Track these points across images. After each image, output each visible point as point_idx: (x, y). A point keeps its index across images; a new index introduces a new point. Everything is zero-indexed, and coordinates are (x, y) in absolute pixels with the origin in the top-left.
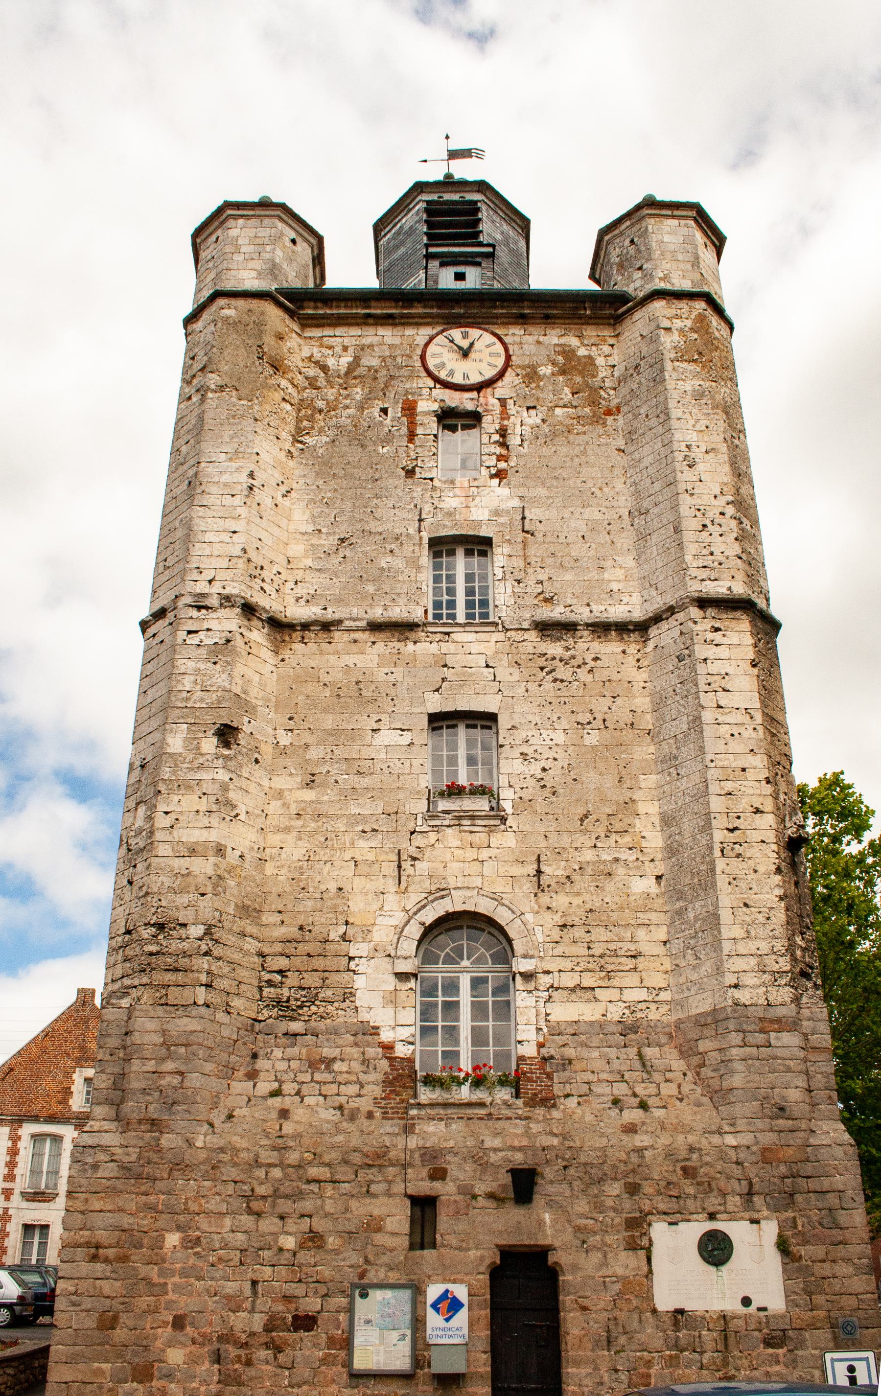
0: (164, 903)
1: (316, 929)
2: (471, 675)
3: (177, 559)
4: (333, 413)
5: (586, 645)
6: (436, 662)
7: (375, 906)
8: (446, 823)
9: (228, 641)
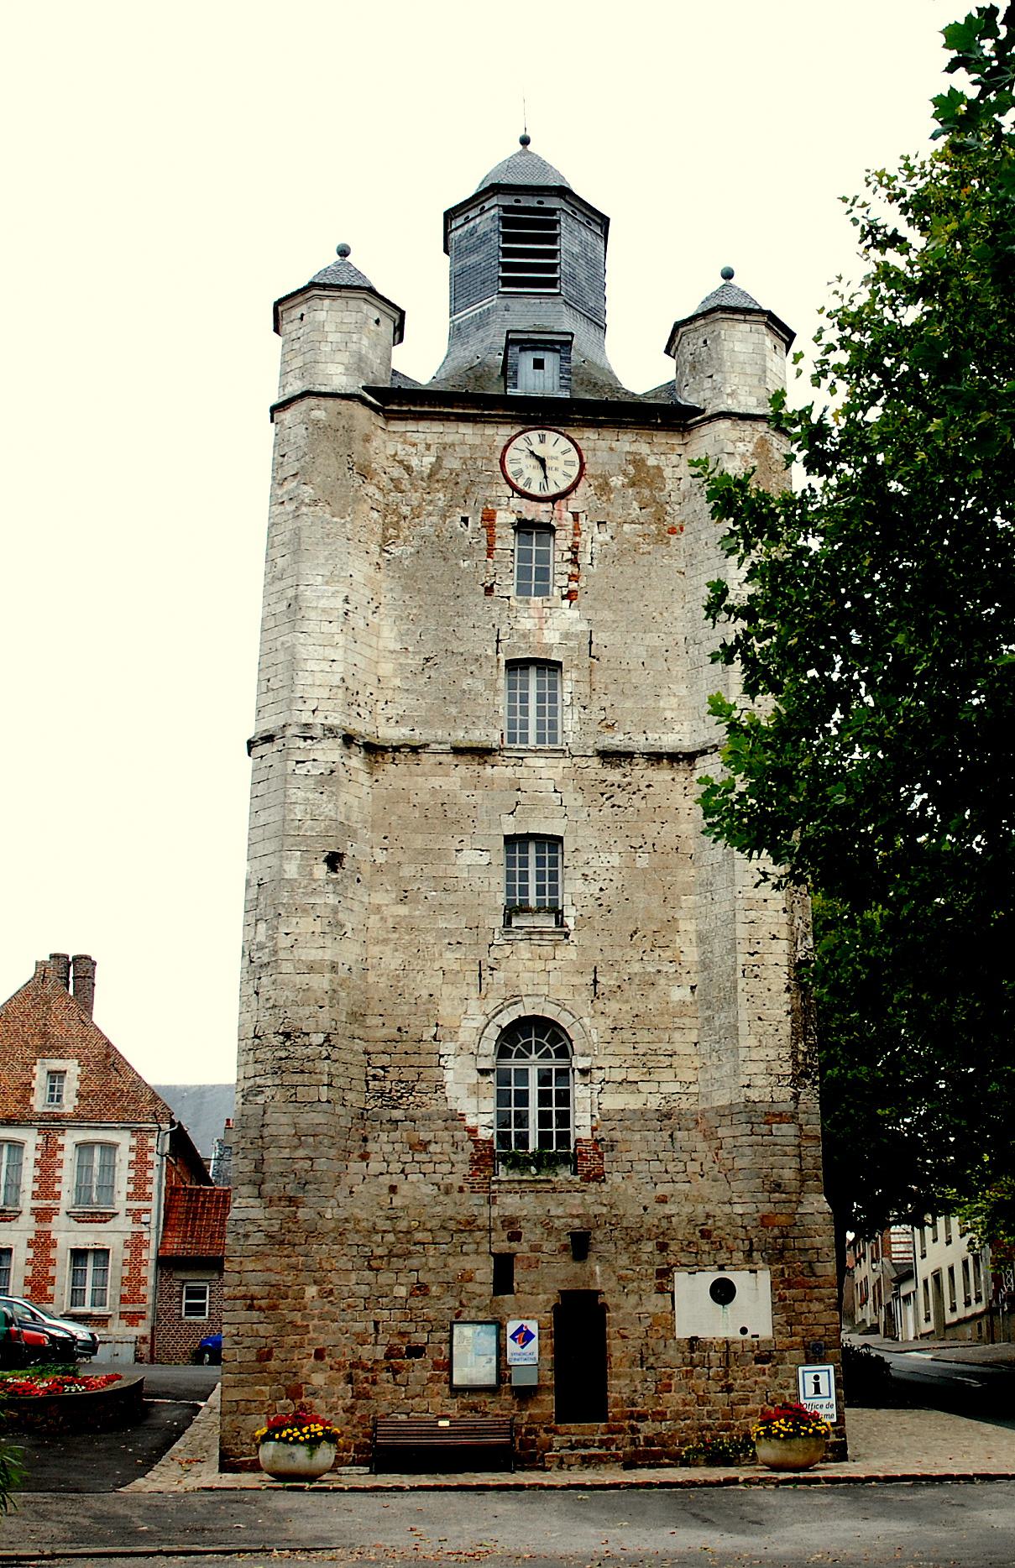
0: (289, 1015)
1: (412, 1031)
2: (542, 799)
3: (281, 684)
4: (417, 520)
5: (641, 773)
6: (512, 786)
7: (461, 1011)
8: (519, 937)
9: (332, 772)
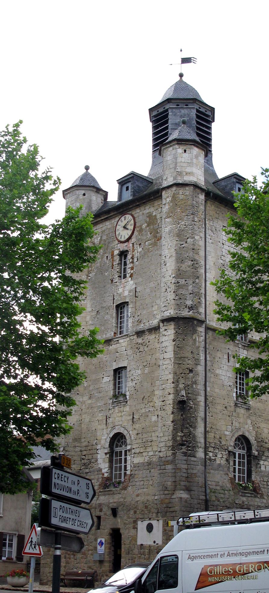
2: (122, 354)
6: (115, 351)
8: (115, 405)
